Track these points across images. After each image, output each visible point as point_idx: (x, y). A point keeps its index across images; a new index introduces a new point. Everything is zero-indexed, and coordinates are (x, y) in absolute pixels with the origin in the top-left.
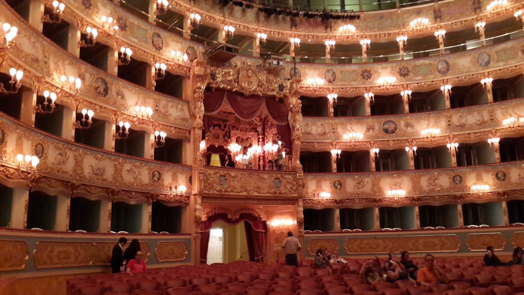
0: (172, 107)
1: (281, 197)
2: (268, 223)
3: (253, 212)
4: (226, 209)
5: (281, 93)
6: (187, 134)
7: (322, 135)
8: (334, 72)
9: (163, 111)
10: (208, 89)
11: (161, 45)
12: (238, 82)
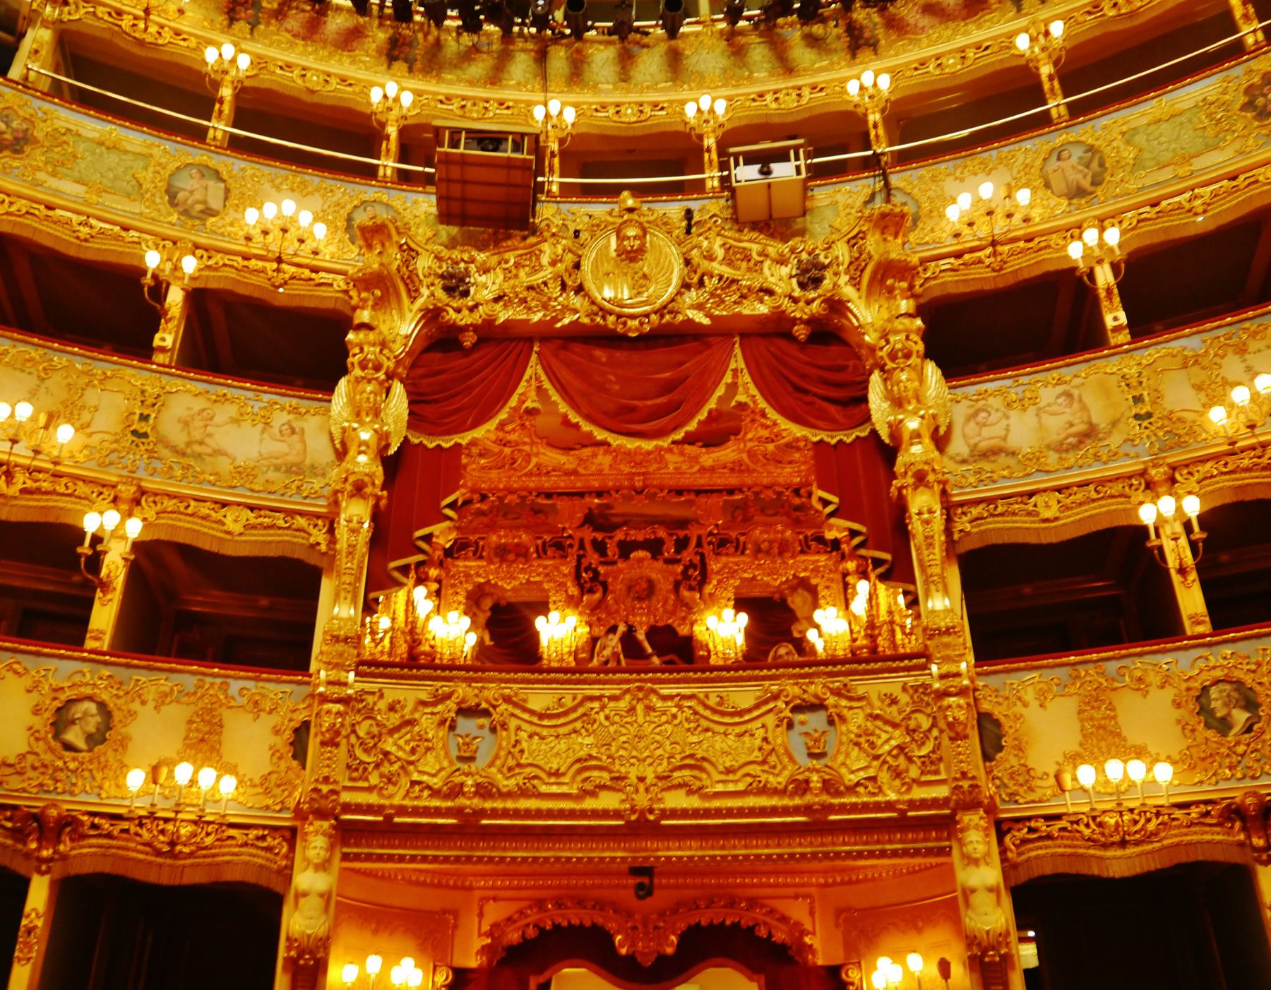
0: (235, 421)
1: (842, 809)
2: (853, 975)
3: (758, 914)
4: (600, 905)
5: (812, 295)
6: (319, 536)
7: (1076, 447)
8: (1091, 149)
9: (178, 437)
10: (439, 338)
11: (215, 203)
12: (580, 289)
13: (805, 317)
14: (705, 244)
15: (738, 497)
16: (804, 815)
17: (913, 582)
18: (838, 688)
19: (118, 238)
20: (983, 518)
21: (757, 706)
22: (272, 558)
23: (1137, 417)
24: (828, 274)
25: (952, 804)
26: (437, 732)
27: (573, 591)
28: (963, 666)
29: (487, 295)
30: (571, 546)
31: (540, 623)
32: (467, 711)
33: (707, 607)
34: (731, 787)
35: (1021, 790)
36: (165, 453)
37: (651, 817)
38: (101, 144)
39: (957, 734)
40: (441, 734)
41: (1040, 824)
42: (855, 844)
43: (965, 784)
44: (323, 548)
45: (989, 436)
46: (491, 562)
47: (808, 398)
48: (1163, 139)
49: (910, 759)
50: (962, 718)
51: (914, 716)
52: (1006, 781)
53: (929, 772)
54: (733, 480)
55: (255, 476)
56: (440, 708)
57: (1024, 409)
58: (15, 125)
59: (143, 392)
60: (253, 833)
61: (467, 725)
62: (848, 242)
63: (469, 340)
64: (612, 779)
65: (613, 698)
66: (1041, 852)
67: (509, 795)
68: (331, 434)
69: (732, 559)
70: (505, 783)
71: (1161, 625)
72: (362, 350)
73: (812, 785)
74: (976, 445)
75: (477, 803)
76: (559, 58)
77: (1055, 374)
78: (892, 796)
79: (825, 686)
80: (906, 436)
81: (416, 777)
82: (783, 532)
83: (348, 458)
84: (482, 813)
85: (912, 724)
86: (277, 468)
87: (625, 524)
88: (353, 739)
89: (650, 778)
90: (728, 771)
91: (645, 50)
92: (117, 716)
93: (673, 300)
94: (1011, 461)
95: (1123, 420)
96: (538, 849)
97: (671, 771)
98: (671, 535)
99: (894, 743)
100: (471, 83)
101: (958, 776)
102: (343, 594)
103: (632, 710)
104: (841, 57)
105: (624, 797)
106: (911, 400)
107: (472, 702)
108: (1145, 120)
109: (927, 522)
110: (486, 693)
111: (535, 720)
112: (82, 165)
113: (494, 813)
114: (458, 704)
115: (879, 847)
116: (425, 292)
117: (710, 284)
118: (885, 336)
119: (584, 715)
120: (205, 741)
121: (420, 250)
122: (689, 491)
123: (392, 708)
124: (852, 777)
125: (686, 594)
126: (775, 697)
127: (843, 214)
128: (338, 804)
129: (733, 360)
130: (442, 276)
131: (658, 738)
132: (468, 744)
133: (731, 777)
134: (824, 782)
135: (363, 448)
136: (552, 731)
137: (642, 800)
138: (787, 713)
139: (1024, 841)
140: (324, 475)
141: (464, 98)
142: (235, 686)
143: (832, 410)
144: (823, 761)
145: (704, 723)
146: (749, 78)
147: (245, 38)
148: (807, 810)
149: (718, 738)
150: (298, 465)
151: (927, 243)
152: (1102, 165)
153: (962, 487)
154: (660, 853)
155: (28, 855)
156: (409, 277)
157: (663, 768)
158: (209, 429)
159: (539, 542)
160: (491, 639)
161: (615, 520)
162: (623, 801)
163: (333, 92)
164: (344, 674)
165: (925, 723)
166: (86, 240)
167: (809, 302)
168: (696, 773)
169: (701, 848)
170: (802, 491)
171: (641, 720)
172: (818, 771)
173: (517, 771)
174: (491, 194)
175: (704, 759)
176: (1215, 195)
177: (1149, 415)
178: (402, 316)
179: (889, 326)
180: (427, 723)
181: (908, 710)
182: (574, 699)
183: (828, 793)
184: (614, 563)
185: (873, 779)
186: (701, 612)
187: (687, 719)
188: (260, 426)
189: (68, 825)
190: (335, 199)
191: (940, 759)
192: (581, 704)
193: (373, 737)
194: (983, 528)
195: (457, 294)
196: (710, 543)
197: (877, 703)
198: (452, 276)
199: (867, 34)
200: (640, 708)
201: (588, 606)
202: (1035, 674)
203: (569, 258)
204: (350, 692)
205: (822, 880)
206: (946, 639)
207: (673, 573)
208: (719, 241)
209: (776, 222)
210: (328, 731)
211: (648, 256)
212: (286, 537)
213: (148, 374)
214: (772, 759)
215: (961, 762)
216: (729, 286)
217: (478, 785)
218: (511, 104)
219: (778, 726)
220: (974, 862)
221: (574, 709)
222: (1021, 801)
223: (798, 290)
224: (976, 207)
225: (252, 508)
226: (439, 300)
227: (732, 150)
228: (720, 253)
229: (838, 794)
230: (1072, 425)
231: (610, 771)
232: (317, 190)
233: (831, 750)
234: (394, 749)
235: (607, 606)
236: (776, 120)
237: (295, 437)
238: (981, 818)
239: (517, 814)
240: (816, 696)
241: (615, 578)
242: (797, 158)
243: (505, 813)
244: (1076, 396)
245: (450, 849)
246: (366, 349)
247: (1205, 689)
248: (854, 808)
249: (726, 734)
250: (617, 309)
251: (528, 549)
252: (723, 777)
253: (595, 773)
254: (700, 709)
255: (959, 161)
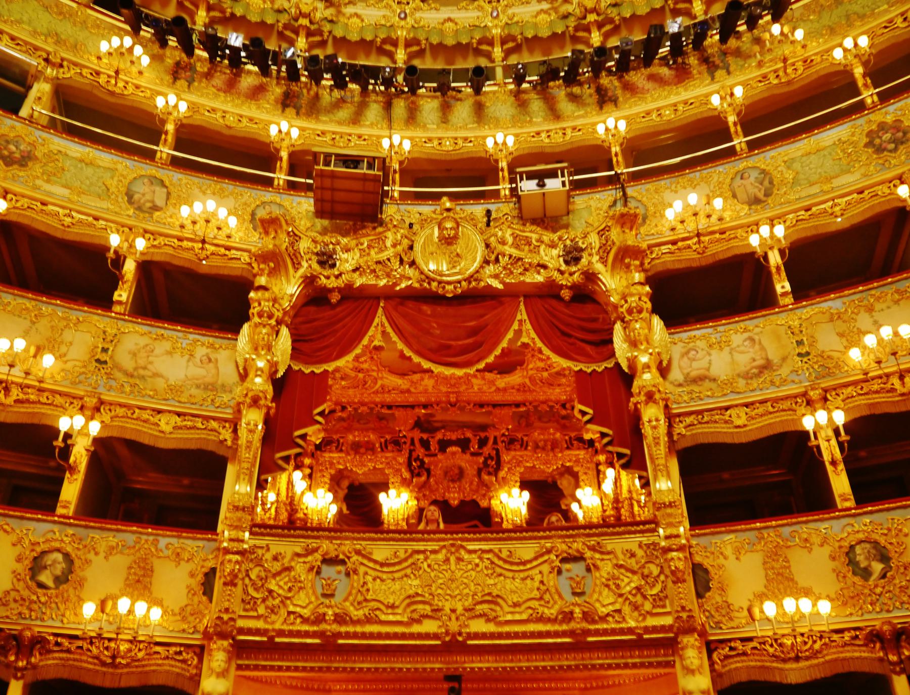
0: (169, 353)
1: (597, 633)
5: (574, 269)
7: (758, 375)
8: (763, 172)
9: (128, 364)
10: (314, 296)
11: (160, 202)
12: (413, 264)
13: (569, 284)
14: (500, 233)
15: (522, 409)
16: (569, 637)
17: (646, 470)
18: (594, 545)
19: (90, 225)
20: (694, 425)
21: (536, 558)
22: (192, 450)
23: (799, 355)
24: (585, 255)
25: (675, 629)
26: (307, 576)
27: (406, 475)
28: (682, 529)
29: (348, 267)
30: (405, 443)
31: (382, 497)
32: (329, 561)
33: (501, 487)
34: (517, 617)
35: (724, 620)
36: (118, 375)
37: (460, 639)
38: (82, 161)
39: (678, 578)
40: (310, 577)
41: (738, 644)
42: (607, 658)
43: (684, 615)
44: (229, 443)
45: (697, 368)
46: (348, 454)
47: (572, 340)
48: (812, 166)
49: (645, 597)
50: (681, 567)
51: (647, 565)
52: (713, 613)
53: (658, 606)
54: (519, 398)
55: (182, 392)
56: (310, 558)
57: (721, 349)
58: (22, 147)
59: (104, 332)
60: (173, 649)
61: (329, 571)
62: (598, 233)
63: (335, 298)
64: (433, 611)
65: (434, 552)
66: (739, 665)
67: (358, 622)
68: (236, 362)
69: (518, 453)
70: (356, 613)
71: (819, 501)
72: (260, 304)
73: (575, 615)
74: (688, 374)
75: (335, 627)
76: (400, 107)
77: (742, 325)
78: (632, 624)
79: (584, 543)
80: (640, 367)
81: (291, 608)
82: (554, 434)
83: (248, 379)
84: (339, 635)
85: (646, 572)
86: (198, 387)
87: (443, 427)
88: (247, 581)
89: (460, 609)
90: (515, 605)
91: (459, 102)
92: (77, 563)
93: (477, 272)
94: (713, 385)
95: (790, 357)
96: (379, 662)
97: (475, 605)
98: (475, 436)
99: (633, 585)
100: (340, 123)
101: (679, 609)
102: (242, 476)
103: (447, 560)
104: (593, 109)
105: (441, 624)
106: (643, 343)
107: (333, 554)
108: (800, 153)
109: (655, 427)
110: (343, 548)
111: (378, 567)
112: (68, 175)
113: (348, 635)
114: (323, 556)
115: (623, 661)
116: (305, 264)
117: (503, 261)
118: (624, 297)
119: (413, 564)
120: (140, 582)
121: (302, 236)
122: (488, 405)
123: (275, 558)
124: (604, 609)
125: (486, 477)
126: (549, 552)
127: (594, 214)
128: (235, 628)
129: (519, 314)
130: (317, 254)
131: (465, 581)
132: (329, 585)
133: (517, 609)
134: (584, 613)
135: (259, 373)
136: (390, 576)
137: (454, 626)
138: (557, 563)
139: (727, 657)
140: (231, 392)
141: (334, 133)
142: (163, 542)
143: (589, 349)
144: (583, 598)
145: (498, 570)
146: (530, 121)
147: (184, 91)
148: (571, 633)
149: (508, 581)
150: (212, 384)
151: (653, 234)
152: (771, 182)
153: (679, 403)
154: (466, 665)
155: (8, 665)
156: (294, 254)
157: (468, 603)
158: (151, 359)
159: (382, 440)
160: (348, 509)
161: (436, 425)
162: (440, 627)
163: (245, 128)
164: (241, 534)
165: (655, 571)
166: (69, 227)
167: (571, 274)
168: (493, 606)
169: (496, 661)
170: (568, 406)
171: (453, 567)
172: (579, 605)
173: (364, 604)
174: (352, 198)
175: (498, 596)
176: (849, 203)
177: (808, 354)
178: (288, 281)
179: (627, 291)
180: (300, 569)
181: (643, 561)
182: (406, 552)
183: (587, 621)
184: (436, 455)
185: (619, 611)
186: (496, 490)
187: (486, 568)
188: (187, 357)
189: (39, 643)
190: (243, 200)
191: (666, 597)
192: (411, 556)
193: (261, 579)
194: (694, 432)
195: (327, 266)
196: (503, 441)
197: (621, 556)
198: (323, 254)
199: (610, 94)
200: (453, 559)
201: (416, 485)
202: (732, 536)
203: (406, 242)
204: (246, 546)
205: (582, 686)
206: (669, 511)
207: (477, 463)
208: (509, 232)
209: (548, 219)
210: (229, 574)
211: (460, 241)
212: (203, 435)
213: (108, 320)
214: (547, 597)
215: (681, 599)
216: (516, 263)
217: (336, 615)
218: (366, 137)
219: (550, 572)
220: (690, 671)
221: (406, 560)
222: (724, 627)
223: (564, 265)
224: (686, 211)
225: (179, 414)
226: (315, 270)
227: (519, 170)
228: (510, 240)
229: (594, 622)
230: (754, 360)
231: (431, 605)
232: (232, 194)
233: (588, 591)
234: (275, 588)
235: (430, 486)
236: (548, 150)
237: (211, 365)
238: (696, 640)
239: (364, 636)
240: (578, 551)
241: (436, 466)
242: (563, 176)
243: (355, 635)
244: (757, 341)
245: (315, 661)
246: (262, 303)
247: (852, 547)
248: (605, 632)
249: (513, 578)
250: (439, 278)
251: (374, 445)
252: (512, 610)
253: (420, 606)
254: (496, 560)
255: (673, 180)
